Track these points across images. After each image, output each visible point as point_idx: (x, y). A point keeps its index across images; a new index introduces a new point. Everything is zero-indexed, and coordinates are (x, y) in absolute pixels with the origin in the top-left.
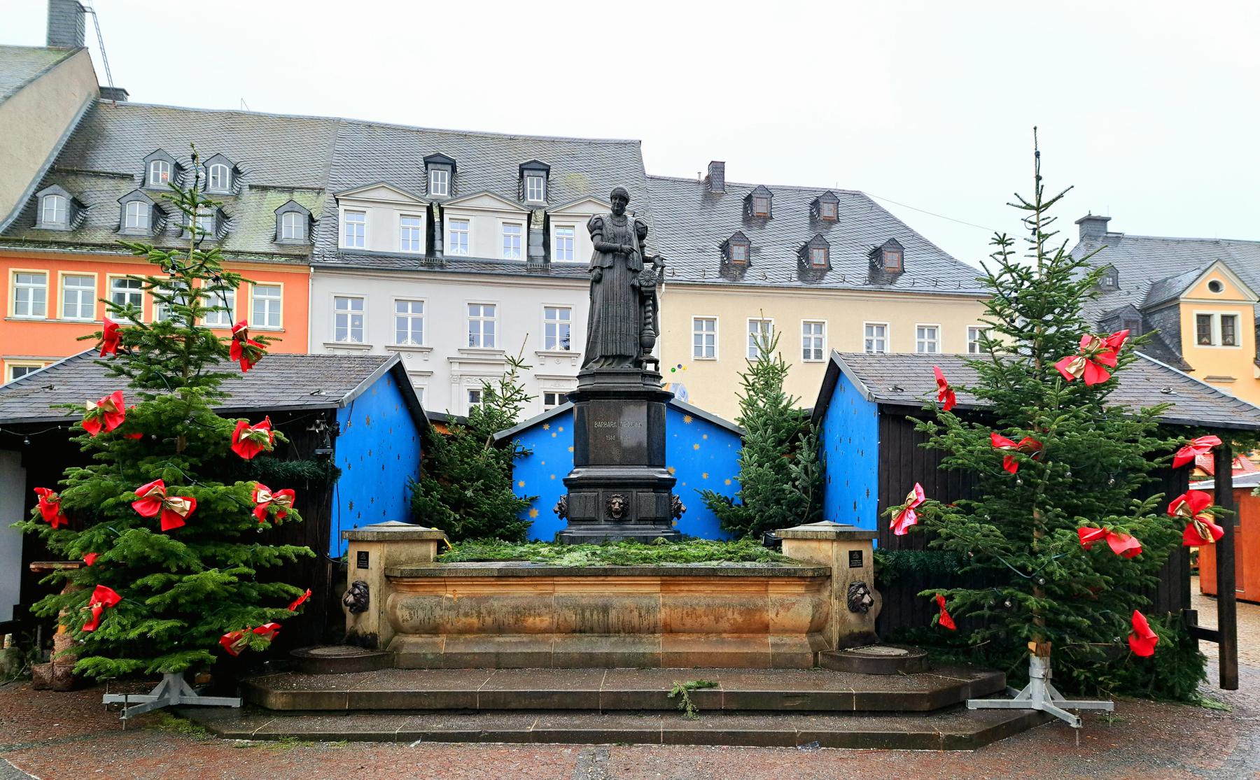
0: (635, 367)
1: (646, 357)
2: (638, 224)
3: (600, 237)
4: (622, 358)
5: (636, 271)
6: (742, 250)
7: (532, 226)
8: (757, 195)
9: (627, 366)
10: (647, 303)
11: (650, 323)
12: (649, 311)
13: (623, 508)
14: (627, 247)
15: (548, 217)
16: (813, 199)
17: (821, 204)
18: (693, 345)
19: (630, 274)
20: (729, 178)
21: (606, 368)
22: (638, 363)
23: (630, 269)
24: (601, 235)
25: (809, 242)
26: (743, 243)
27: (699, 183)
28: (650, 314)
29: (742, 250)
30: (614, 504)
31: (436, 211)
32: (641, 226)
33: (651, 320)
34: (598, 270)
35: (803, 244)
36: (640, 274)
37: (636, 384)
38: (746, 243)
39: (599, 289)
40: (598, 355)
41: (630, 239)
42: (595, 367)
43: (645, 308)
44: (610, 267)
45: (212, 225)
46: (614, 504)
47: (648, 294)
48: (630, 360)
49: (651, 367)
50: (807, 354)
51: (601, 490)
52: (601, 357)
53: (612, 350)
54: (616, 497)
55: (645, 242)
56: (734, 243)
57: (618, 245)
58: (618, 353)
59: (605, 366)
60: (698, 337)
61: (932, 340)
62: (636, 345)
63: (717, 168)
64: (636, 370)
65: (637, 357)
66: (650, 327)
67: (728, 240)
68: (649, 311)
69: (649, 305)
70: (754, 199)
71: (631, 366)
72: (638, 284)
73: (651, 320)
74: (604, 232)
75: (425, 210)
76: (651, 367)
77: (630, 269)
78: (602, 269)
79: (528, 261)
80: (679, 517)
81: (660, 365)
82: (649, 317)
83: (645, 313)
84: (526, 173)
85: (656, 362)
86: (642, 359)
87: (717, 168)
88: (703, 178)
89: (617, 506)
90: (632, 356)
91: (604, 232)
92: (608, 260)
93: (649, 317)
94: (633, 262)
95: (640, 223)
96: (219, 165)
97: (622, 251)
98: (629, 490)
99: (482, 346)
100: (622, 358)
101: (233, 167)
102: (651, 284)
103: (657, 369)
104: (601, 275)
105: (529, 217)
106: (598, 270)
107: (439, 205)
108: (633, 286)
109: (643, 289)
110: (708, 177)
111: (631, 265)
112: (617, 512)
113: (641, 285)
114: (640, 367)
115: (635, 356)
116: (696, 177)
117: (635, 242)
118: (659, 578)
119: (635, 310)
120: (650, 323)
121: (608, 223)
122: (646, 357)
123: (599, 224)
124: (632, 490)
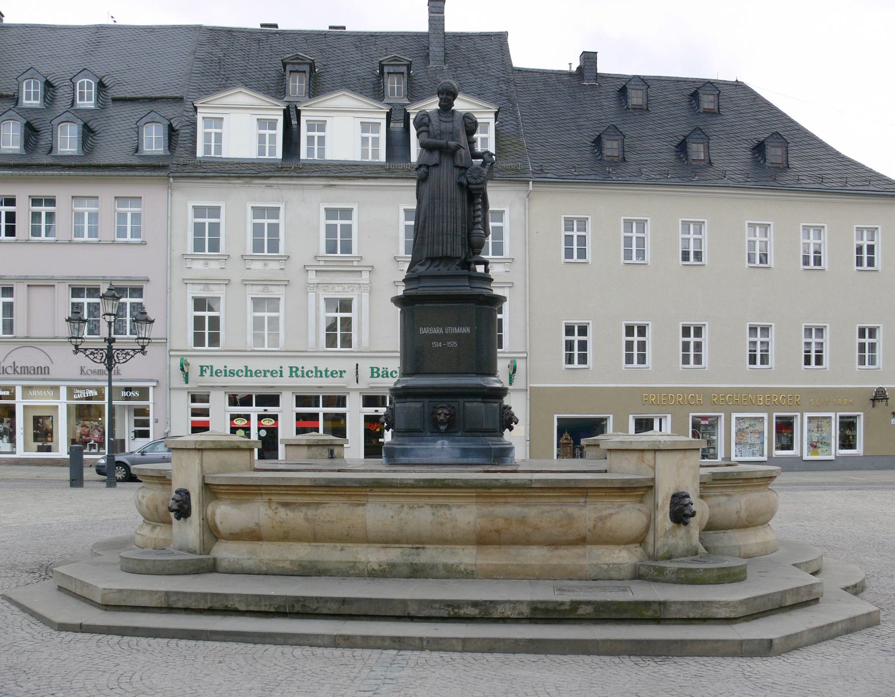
0: (463, 269)
1: (475, 259)
2: (466, 119)
4: (447, 259)
5: (465, 168)
6: (615, 144)
7: (392, 125)
8: (631, 86)
9: (454, 269)
10: (476, 202)
11: (479, 223)
12: (479, 210)
13: (449, 419)
14: (452, 143)
16: (693, 91)
17: (701, 95)
18: (563, 247)
19: (457, 172)
21: (433, 270)
22: (467, 264)
23: (457, 167)
24: (428, 132)
25: (688, 136)
26: (616, 138)
27: (570, 74)
28: (480, 213)
29: (615, 144)
30: (440, 414)
31: (293, 114)
32: (470, 121)
33: (480, 219)
35: (682, 138)
36: (468, 172)
37: (463, 288)
38: (619, 137)
39: (426, 187)
40: (425, 256)
41: (458, 136)
42: (421, 270)
43: (474, 206)
44: (436, 165)
45: (78, 141)
46: (440, 414)
48: (458, 262)
49: (480, 269)
50: (685, 256)
51: (426, 400)
52: (427, 259)
53: (439, 251)
54: (443, 407)
56: (606, 137)
57: (444, 142)
58: (445, 254)
60: (569, 239)
61: (764, 239)
62: (463, 245)
63: (589, 58)
64: (466, 272)
65: (466, 258)
66: (480, 226)
67: (599, 136)
68: (479, 210)
69: (479, 203)
70: (629, 91)
71: (459, 268)
72: (465, 182)
73: (480, 219)
75: (282, 113)
76: (480, 269)
77: (457, 167)
78: (428, 167)
79: (386, 162)
80: (511, 429)
82: (479, 216)
83: (474, 212)
84: (386, 70)
85: (486, 263)
86: (470, 260)
87: (589, 58)
88: (574, 69)
89: (442, 417)
90: (459, 258)
91: (431, 128)
92: (435, 157)
93: (479, 216)
94: (461, 159)
95: (469, 118)
96: (86, 80)
97: (448, 147)
98: (457, 399)
100: (447, 259)
101: (98, 80)
102: (479, 181)
103: (487, 270)
104: (427, 174)
105: (389, 116)
106: (423, 169)
107: (296, 107)
108: (460, 184)
109: (471, 187)
110: (579, 68)
111: (458, 163)
112: (442, 423)
113: (469, 183)
114: (469, 269)
115: (463, 258)
116: (567, 68)
117: (463, 140)
118: (474, 490)
119: (463, 210)
120: (479, 223)
121: (435, 120)
122: (475, 259)
123: (426, 120)
124: (460, 400)
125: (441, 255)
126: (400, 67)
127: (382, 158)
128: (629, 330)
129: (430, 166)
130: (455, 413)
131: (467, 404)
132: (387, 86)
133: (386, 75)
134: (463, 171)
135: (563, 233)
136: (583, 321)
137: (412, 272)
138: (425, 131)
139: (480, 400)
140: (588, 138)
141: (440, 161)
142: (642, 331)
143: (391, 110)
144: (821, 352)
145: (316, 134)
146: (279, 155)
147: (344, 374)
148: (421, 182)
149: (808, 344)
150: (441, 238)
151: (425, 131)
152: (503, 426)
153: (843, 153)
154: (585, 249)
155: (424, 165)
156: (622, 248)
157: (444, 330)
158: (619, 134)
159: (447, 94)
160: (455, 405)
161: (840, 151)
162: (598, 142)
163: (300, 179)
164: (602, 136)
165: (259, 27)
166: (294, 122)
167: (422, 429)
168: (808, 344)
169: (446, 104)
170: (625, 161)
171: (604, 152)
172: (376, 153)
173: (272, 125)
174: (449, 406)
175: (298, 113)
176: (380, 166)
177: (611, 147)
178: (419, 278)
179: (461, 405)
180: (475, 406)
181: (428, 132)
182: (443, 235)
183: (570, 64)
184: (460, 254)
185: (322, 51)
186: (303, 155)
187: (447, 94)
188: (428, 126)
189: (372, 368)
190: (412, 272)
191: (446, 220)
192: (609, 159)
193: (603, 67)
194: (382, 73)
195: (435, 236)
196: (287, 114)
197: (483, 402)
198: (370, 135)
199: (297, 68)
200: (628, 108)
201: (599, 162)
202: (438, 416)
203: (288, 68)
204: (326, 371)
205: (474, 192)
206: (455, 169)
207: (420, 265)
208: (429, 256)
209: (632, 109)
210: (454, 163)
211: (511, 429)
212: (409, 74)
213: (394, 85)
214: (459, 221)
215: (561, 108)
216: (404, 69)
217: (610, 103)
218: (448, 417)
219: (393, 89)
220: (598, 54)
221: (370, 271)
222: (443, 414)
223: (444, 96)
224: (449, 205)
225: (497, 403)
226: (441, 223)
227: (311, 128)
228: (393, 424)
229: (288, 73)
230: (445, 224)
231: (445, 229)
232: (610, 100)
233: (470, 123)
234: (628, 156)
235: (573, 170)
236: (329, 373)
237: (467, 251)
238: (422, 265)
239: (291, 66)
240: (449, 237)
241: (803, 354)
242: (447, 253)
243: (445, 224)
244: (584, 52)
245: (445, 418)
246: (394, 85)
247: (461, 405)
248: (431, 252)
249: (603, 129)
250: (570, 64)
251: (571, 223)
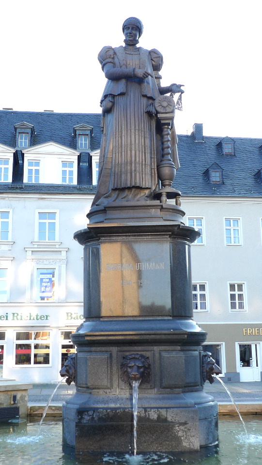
3: (112, 64)
6: (218, 174)
7: (81, 164)
15: (91, 156)
19: (144, 100)
20: (206, 133)
23: (145, 96)
26: (218, 170)
27: (187, 136)
29: (218, 174)
31: (20, 157)
34: (110, 98)
44: (122, 94)
47: (167, 122)
51: (114, 350)
55: (160, 73)
56: (212, 170)
58: (133, 184)
63: (198, 128)
64: (157, 202)
70: (223, 144)
72: (154, 111)
74: (116, 60)
75: (12, 155)
77: (145, 96)
78: (114, 96)
84: (78, 133)
87: (198, 128)
92: (121, 87)
99: (47, 241)
105: (79, 157)
107: (21, 152)
109: (159, 116)
113: (157, 112)
124: (155, 348)
125: (129, 186)
126: (87, 131)
127: (75, 182)
128: (232, 287)
129: (117, 96)
130: (149, 365)
131: (164, 354)
132: (78, 143)
133: (77, 136)
134: (151, 101)
136: (202, 282)
137: (97, 205)
138: (110, 62)
139: (179, 348)
140: (200, 172)
141: (127, 90)
142: (240, 287)
143: (80, 154)
145: (34, 168)
146: (10, 180)
147: (48, 318)
148: (105, 114)
150: (129, 168)
151: (110, 62)
152: (203, 378)
155: (111, 94)
156: (225, 236)
158: (219, 168)
159: (133, 28)
160: (148, 354)
162: (206, 174)
163: (23, 194)
164: (210, 170)
165: (2, 110)
166: (20, 162)
167: (109, 386)
169: (131, 39)
170: (224, 184)
171: (211, 179)
172: (71, 179)
173: (6, 162)
174: (142, 356)
175: (23, 155)
176: (74, 187)
177: (215, 177)
178: (105, 210)
179: (157, 355)
180: (173, 356)
181: (114, 64)
182: (131, 164)
184: (150, 184)
185: (39, 123)
186: (25, 180)
187: (133, 28)
188: (113, 58)
189: (67, 313)
190: (97, 205)
191: (133, 149)
192: (214, 183)
193: (206, 133)
194: (75, 135)
195: (123, 166)
196: (16, 156)
197: (182, 350)
198: (68, 169)
199: (23, 131)
200: (223, 155)
202: (129, 370)
203: (18, 131)
204: (37, 316)
205: (162, 122)
206: (142, 98)
207: (106, 197)
208: (115, 187)
209: (226, 155)
210: (141, 92)
211: (212, 380)
212: (91, 135)
213: (83, 142)
214: (148, 151)
216: (88, 132)
217: (212, 152)
218: (142, 370)
219: (81, 144)
221: (67, 251)
222: (135, 368)
223: (129, 31)
224: (137, 133)
225: (197, 350)
226: (129, 152)
227: (30, 164)
228: (74, 378)
229: (17, 134)
230: (133, 152)
231: (133, 159)
233: (156, 57)
234: (225, 181)
236: (39, 317)
237: (157, 182)
239: (19, 129)
240: (137, 165)
242: (135, 183)
243: (133, 152)
245: (138, 371)
246: (83, 142)
247: (157, 355)
248: (118, 180)
249: (208, 166)
251: (192, 221)
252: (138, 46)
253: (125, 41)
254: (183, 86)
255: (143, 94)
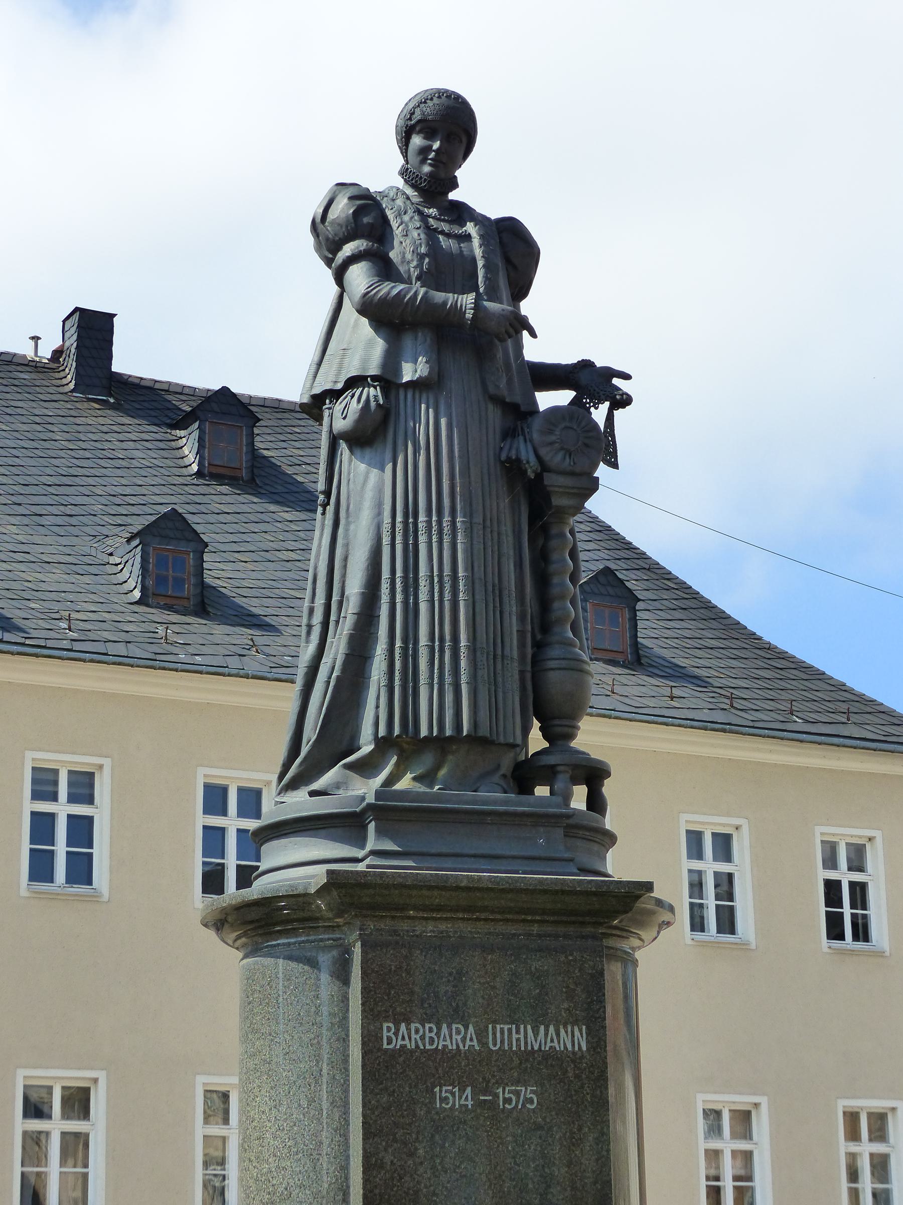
18: (26, 846)
27: (34, 366)
52: (384, 744)
59: (405, 783)
81: (608, 788)
88: (45, 352)
103: (596, 803)
113: (544, 467)
116: (26, 350)
135: (29, 806)
137: (313, 794)
144: (750, 1178)
149: (714, 1156)
153: (766, 638)
154: (91, 855)
157: (481, 1035)
161: (759, 633)
168: (714, 1156)
183: (36, 339)
201: (136, 608)
215: (14, 452)
220: (115, 319)
232: (148, 445)
235: (64, 625)
238: (365, 768)
241: (703, 1183)
244: (77, 309)
250: (36, 339)
252: (453, 196)
253: (404, 172)
254: (627, 377)
255: (492, 390)
